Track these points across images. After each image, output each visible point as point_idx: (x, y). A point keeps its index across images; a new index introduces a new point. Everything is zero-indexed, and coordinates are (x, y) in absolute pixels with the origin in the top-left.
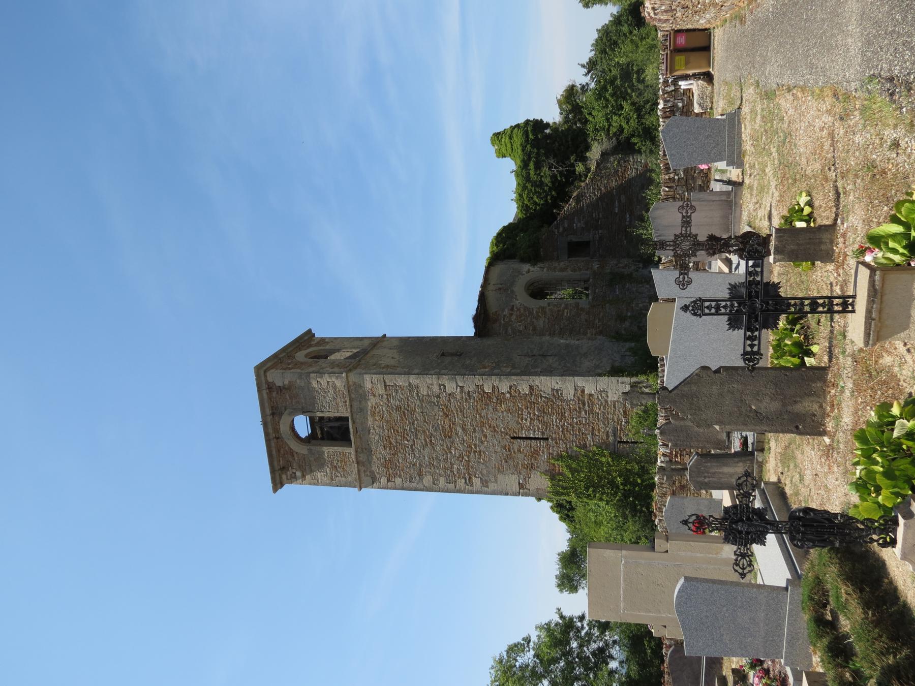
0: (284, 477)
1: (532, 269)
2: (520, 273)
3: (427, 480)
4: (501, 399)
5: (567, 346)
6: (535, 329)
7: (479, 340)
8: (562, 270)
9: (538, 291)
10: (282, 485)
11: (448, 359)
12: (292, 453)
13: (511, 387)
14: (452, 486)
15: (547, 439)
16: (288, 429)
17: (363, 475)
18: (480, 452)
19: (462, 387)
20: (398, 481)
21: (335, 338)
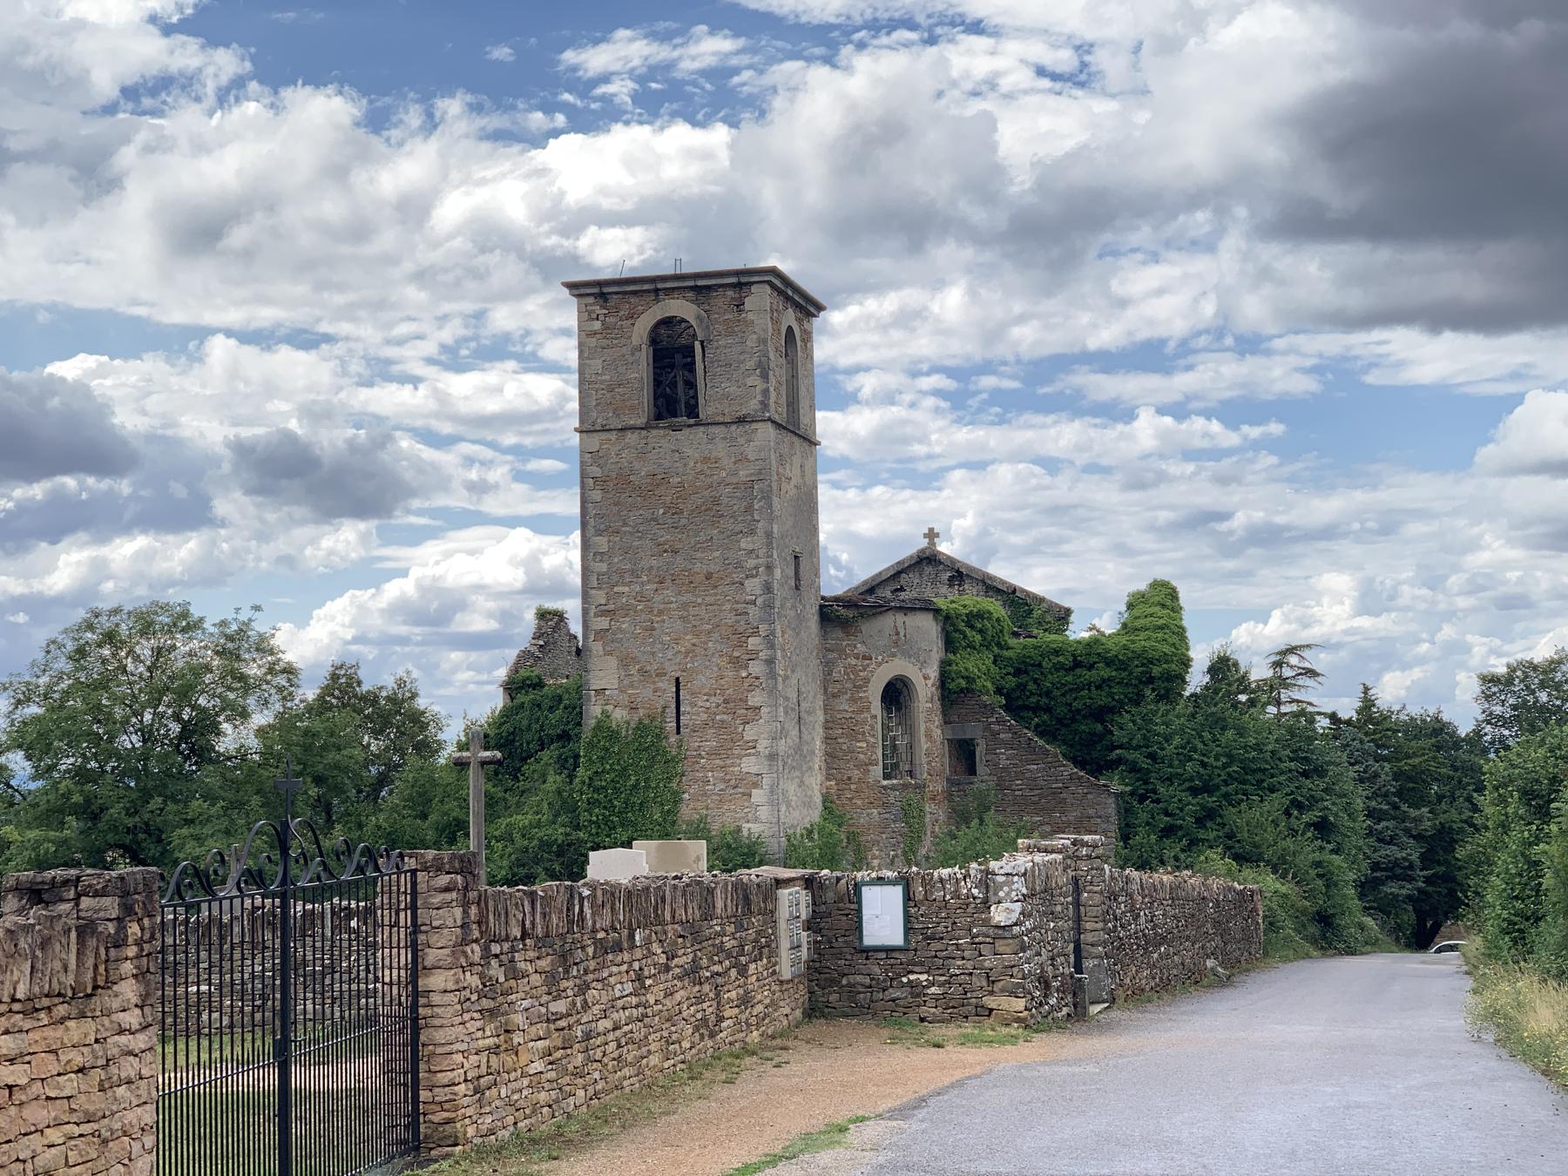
0: (591, 300)
1: (930, 683)
3: (602, 543)
8: (929, 736)
9: (896, 694)
15: (678, 732)
17: (604, 436)
18: (653, 629)
20: (596, 495)
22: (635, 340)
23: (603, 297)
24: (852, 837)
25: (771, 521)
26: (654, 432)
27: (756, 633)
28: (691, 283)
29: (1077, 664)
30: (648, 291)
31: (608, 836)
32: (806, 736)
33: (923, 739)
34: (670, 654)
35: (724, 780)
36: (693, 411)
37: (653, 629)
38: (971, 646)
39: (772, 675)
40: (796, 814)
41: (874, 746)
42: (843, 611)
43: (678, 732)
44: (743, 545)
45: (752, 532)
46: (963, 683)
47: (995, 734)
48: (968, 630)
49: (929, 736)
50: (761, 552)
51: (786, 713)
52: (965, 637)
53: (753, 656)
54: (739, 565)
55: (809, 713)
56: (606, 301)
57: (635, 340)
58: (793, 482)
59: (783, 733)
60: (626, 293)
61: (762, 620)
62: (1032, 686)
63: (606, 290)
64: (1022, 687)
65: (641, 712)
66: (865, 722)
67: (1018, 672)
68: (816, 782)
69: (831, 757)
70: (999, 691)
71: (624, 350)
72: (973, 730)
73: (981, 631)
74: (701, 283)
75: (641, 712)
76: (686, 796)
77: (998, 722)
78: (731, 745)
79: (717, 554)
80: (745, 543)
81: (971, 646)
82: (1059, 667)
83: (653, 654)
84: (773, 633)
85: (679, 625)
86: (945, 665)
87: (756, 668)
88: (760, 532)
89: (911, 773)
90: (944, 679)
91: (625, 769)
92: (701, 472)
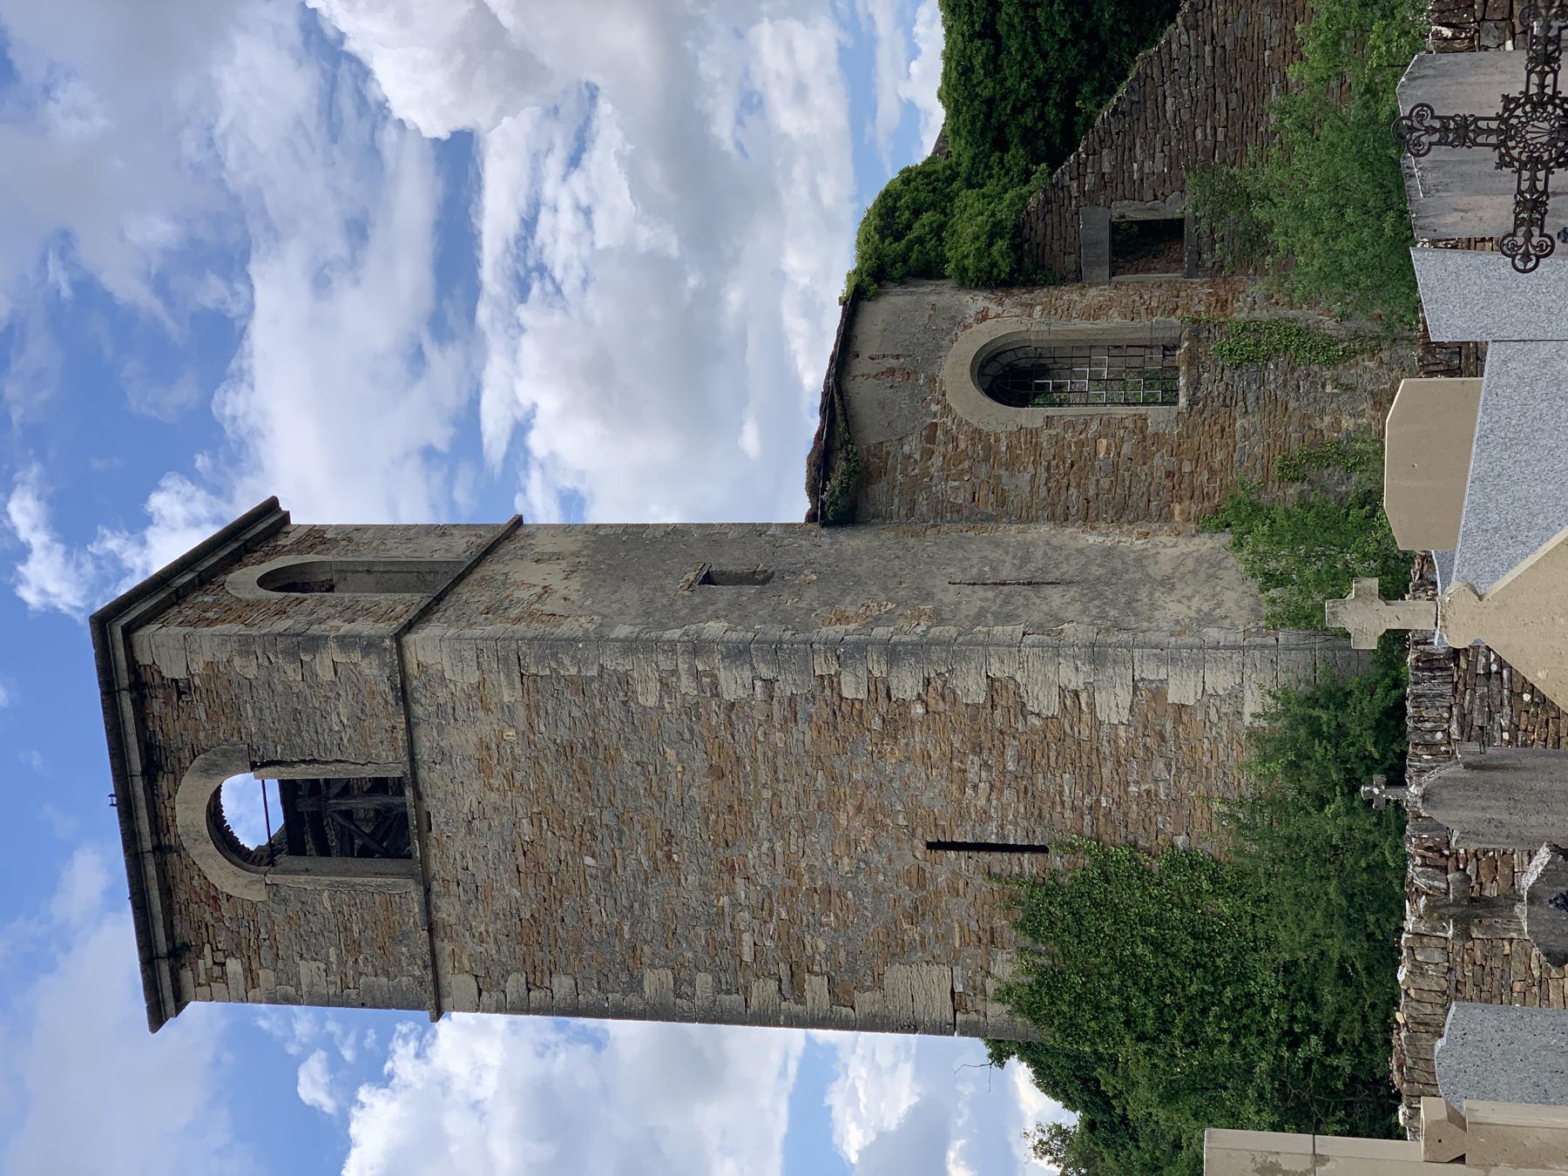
0: (187, 976)
1: (994, 309)
2: (957, 321)
3: (655, 981)
4: (896, 723)
5: (1108, 553)
6: (1002, 501)
7: (825, 537)
8: (1096, 312)
9: (1012, 377)
10: (180, 1005)
11: (724, 593)
12: (214, 898)
13: (927, 682)
14: (738, 999)
15: (1043, 849)
16: (201, 818)
17: (446, 965)
18: (828, 890)
19: (769, 683)
20: (562, 985)
21: (358, 529)
22: (258, 894)
23: (179, 953)
24: (1292, 471)
25: (601, 640)
26: (434, 866)
27: (833, 682)
28: (139, 786)
29: (988, 31)
30: (162, 868)
31: (1266, 1011)
32: (1069, 570)
33: (1103, 324)
34: (878, 859)
35: (1147, 761)
36: (397, 786)
37: (828, 890)
38: (938, 231)
39: (920, 650)
40: (1229, 597)
41: (1106, 423)
42: (834, 483)
43: (1043, 849)
44: (651, 701)
45: (625, 680)
46: (1001, 244)
47: (1103, 182)
48: (911, 236)
49: (1096, 312)
50: (666, 664)
51: (1009, 618)
52: (920, 240)
53: (881, 690)
54: (692, 711)
55: (1026, 559)
56: (186, 947)
57: (258, 894)
58: (556, 582)
59: (1050, 627)
60: (168, 911)
61: (806, 669)
62: (1027, 119)
63: (162, 946)
64: (1028, 136)
65: (1000, 922)
66: (1057, 440)
67: (1002, 145)
68: (1173, 547)
69: (1123, 511)
70: (1026, 177)
71: (279, 917)
72: (1094, 225)
73: (917, 213)
74: (136, 765)
75: (1000, 922)
76: (1180, 841)
77: (1080, 176)
78: (1068, 740)
79: (671, 754)
80: (648, 698)
81: (938, 231)
82: (993, 64)
83: (877, 892)
84: (832, 646)
85: (819, 839)
86: (967, 281)
87: (906, 684)
88: (624, 665)
89: (1169, 348)
90: (990, 281)
91: (1121, 965)
92: (510, 777)
